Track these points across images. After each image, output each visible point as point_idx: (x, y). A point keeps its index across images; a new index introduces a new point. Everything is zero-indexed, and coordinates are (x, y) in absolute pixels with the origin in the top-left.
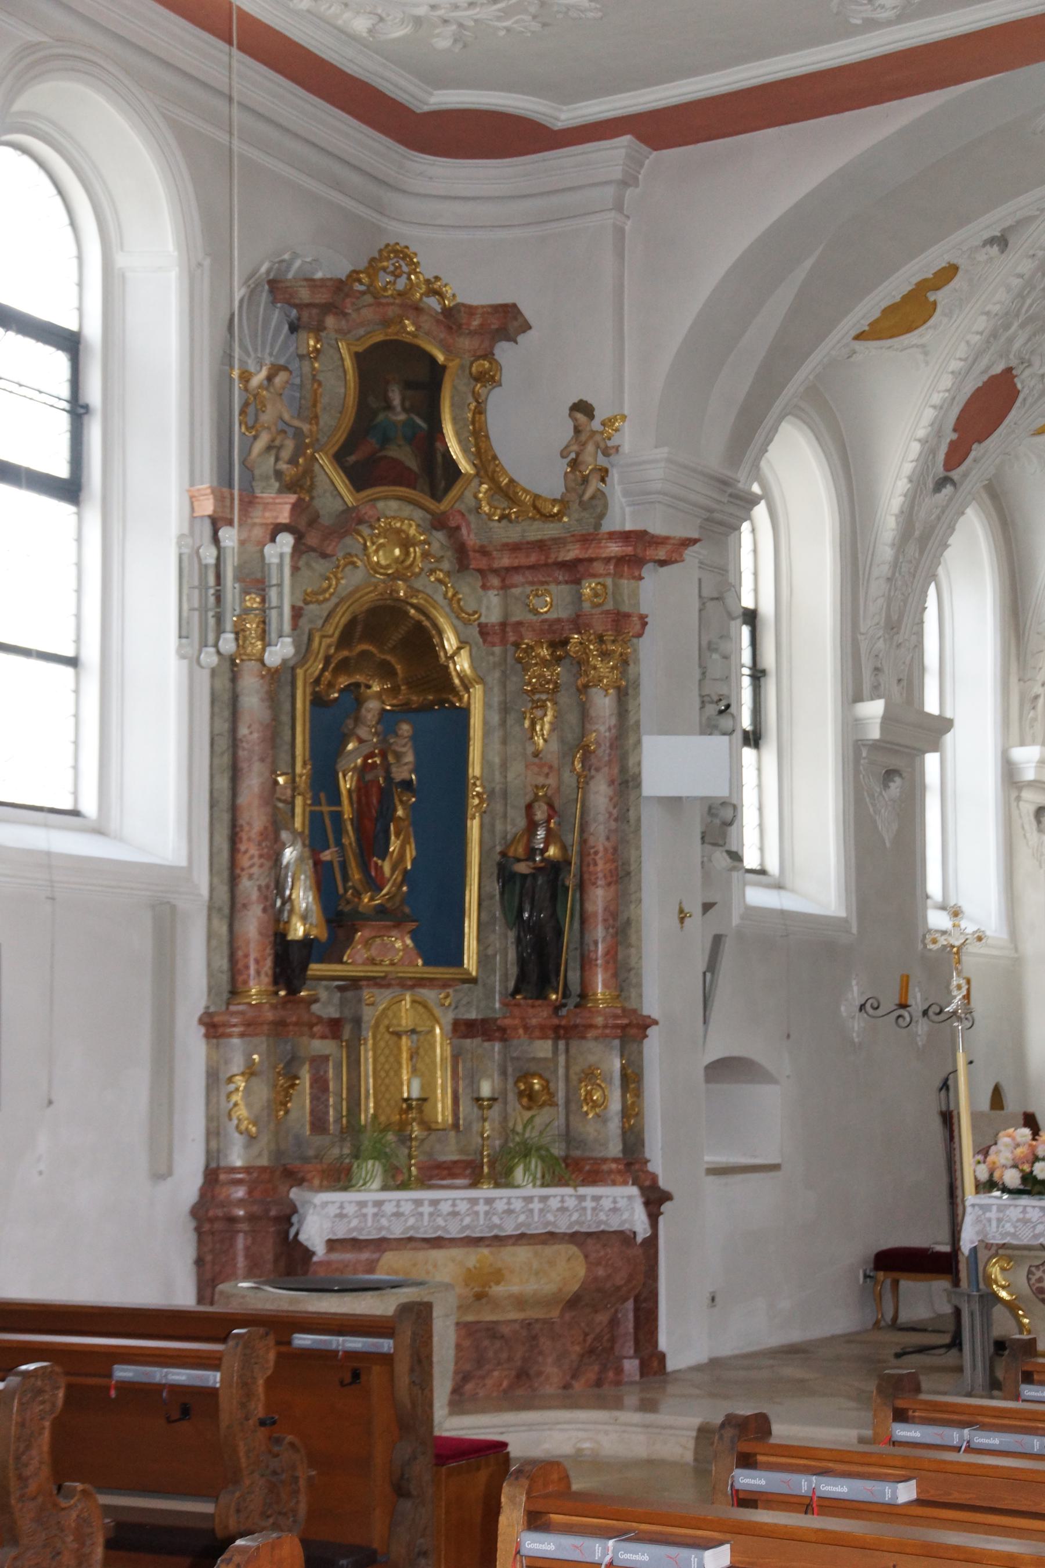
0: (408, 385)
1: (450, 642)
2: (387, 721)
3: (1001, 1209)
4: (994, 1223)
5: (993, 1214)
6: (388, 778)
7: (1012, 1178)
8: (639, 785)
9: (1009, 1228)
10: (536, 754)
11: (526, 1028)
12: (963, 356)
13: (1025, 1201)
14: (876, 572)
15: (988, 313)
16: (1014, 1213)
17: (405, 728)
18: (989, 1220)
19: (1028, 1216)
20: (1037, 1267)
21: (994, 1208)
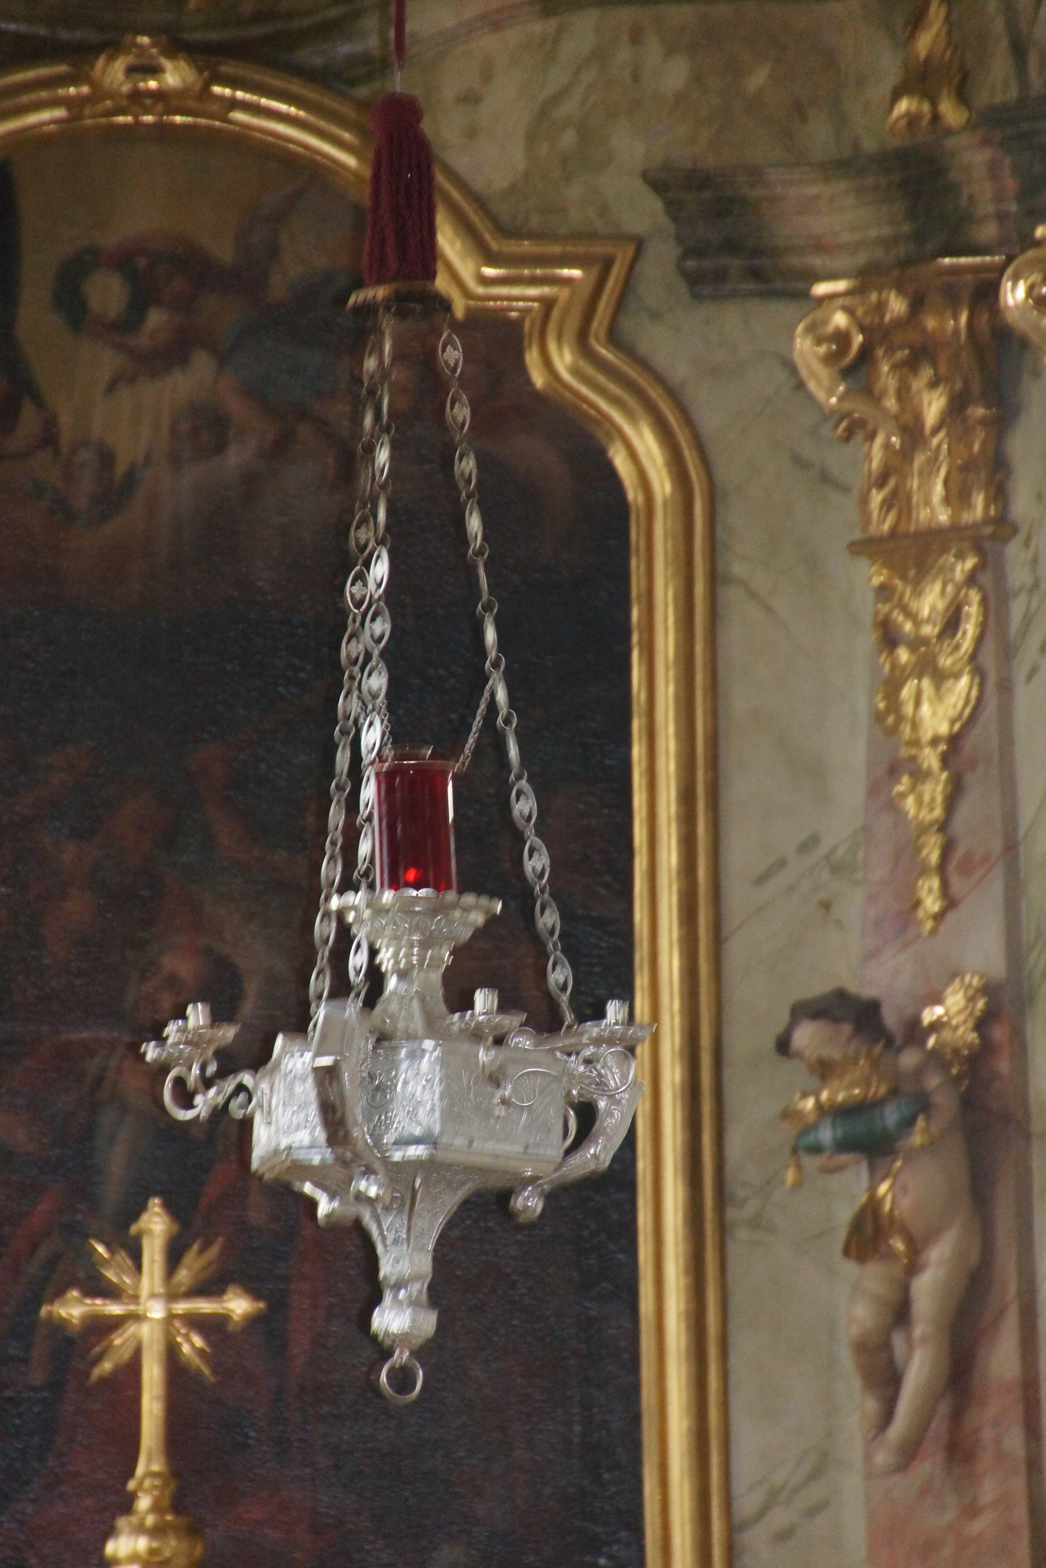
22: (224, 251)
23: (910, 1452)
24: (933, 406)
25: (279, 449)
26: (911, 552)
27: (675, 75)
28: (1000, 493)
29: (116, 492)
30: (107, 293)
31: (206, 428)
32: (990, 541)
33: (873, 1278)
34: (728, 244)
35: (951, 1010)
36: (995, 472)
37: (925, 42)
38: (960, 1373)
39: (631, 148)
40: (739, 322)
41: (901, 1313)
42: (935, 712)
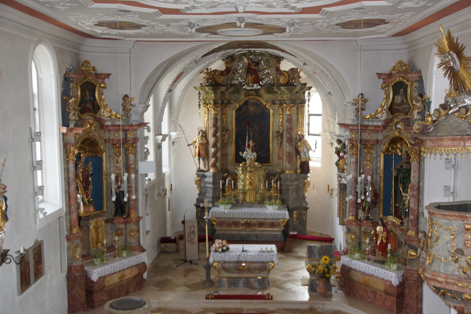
0: (90, 90)
1: (100, 145)
2: (87, 161)
6: (88, 174)
7: (220, 250)
8: (138, 172)
9: (219, 258)
10: (117, 166)
11: (119, 222)
13: (221, 254)
14: (159, 109)
17: (91, 163)
26: (280, 114)
29: (251, 112)
31: (255, 109)
32: (283, 114)
34: (274, 103)
35: (281, 131)
38: (281, 144)
39: (270, 99)
40: (274, 105)
42: (281, 120)
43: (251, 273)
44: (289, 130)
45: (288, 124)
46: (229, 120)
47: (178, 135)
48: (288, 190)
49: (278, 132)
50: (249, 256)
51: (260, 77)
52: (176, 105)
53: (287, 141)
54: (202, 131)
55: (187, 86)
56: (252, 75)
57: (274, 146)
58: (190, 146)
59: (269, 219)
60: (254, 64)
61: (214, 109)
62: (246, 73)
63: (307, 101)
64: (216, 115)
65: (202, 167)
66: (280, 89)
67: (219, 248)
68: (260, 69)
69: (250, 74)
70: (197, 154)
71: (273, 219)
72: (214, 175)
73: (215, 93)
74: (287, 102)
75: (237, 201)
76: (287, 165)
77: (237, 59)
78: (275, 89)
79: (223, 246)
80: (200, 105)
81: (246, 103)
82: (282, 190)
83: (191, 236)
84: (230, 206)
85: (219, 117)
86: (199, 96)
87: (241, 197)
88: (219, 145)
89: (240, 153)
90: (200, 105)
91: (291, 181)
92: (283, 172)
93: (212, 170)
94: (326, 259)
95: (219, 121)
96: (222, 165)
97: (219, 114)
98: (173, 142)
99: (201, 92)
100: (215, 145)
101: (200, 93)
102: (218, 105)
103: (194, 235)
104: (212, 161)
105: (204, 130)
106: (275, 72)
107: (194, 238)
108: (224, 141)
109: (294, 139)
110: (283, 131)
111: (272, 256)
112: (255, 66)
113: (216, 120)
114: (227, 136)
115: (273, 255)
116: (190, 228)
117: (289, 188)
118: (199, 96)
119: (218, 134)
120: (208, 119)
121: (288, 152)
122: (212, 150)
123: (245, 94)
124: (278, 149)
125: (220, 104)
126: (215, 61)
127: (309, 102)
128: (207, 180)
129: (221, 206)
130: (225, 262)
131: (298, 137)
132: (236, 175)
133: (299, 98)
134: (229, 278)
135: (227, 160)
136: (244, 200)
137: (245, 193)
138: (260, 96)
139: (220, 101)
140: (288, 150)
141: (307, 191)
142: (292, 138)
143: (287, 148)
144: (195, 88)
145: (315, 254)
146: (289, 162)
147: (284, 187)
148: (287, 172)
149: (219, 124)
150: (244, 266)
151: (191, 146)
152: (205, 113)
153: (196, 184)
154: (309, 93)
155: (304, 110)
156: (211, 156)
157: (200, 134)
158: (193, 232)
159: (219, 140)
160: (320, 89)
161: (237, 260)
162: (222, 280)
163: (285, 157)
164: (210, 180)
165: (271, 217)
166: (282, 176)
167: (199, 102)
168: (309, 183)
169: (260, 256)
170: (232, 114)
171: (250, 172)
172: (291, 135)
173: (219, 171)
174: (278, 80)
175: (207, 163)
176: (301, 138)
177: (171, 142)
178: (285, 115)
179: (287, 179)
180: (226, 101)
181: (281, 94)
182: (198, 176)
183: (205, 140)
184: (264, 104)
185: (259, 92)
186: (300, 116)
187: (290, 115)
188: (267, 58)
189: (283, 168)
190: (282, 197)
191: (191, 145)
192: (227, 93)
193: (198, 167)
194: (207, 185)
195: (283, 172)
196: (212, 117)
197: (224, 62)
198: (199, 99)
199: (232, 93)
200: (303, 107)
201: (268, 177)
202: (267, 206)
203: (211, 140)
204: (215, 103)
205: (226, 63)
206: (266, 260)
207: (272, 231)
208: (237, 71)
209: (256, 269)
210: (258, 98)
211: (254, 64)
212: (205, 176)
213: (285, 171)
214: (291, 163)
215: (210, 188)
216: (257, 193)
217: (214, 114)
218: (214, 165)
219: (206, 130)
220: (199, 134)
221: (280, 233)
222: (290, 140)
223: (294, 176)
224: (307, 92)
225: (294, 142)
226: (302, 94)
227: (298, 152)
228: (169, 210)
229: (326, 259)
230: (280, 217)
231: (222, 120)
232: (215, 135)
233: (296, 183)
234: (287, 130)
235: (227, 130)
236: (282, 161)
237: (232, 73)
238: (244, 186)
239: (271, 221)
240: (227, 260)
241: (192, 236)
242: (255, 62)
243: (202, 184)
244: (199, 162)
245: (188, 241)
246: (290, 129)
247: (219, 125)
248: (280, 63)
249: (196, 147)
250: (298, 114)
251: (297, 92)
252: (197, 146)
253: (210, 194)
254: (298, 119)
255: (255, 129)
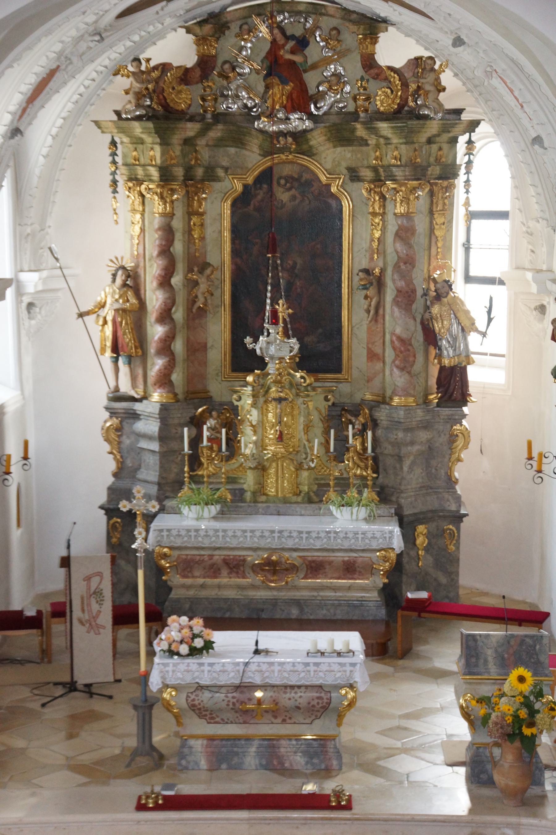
3: (175, 665)
4: (171, 673)
5: (170, 668)
7: (184, 649)
9: (179, 675)
12: (44, 65)
13: (190, 660)
15: (62, 42)
16: (182, 667)
18: (167, 672)
19: (190, 668)
20: (192, 693)
21: (171, 665)
22: (296, 176)
23: (370, 322)
24: (377, 198)
25: (302, 201)
26: (374, 214)
27: (349, 155)
28: (384, 209)
29: (283, 206)
30: (283, 182)
31: (294, 198)
33: (367, 302)
34: (354, 175)
35: (377, 270)
36: (383, 206)
37: (378, 153)
39: (344, 164)
40: (356, 185)
41: (370, 305)
42: (377, 234)
43: (284, 721)
44: (403, 267)
45: (399, 246)
46: (210, 232)
47: (45, 281)
48: (400, 459)
49: (367, 271)
50: (276, 668)
51: (312, 91)
52: (35, 181)
53: (396, 302)
54: (123, 268)
55: (71, 120)
56: (284, 82)
57: (355, 320)
58: (86, 318)
59: (340, 550)
60: (291, 44)
61: (162, 197)
62: (266, 77)
63: (463, 170)
64: (169, 216)
65: (125, 387)
66: (374, 131)
67: (181, 642)
68: (310, 62)
69: (276, 80)
70: (109, 344)
71: (352, 550)
72: (164, 409)
73: (165, 143)
74: (398, 173)
75: (239, 495)
76: (395, 378)
77: (234, 28)
78: (360, 131)
79: (195, 636)
80: (115, 183)
81: (266, 177)
82: (381, 458)
83: (89, 605)
84: (214, 509)
85: (177, 224)
86: (114, 154)
87: (249, 481)
88: (179, 314)
89: (248, 340)
90: (115, 183)
91: (408, 430)
92: (383, 400)
93: (156, 396)
94: (521, 679)
95: (178, 236)
96: (189, 379)
97: (179, 212)
98: (30, 305)
99: (117, 139)
100: (165, 316)
101: (113, 143)
102: (175, 186)
103: (100, 602)
104: (157, 368)
105: (129, 265)
106: (360, 72)
107: (100, 612)
108: (194, 302)
109: (419, 292)
110: (383, 271)
111: (348, 668)
112: (293, 52)
113: (168, 233)
114: (203, 287)
115: (353, 665)
116: (88, 579)
117: (404, 451)
118: (114, 154)
119: (177, 280)
120: (143, 230)
121: (400, 339)
122: (156, 332)
123: (261, 147)
124: (369, 329)
125: (184, 179)
126: (161, 35)
127: (468, 173)
128: (140, 426)
129: (185, 510)
130: (201, 687)
131: (433, 288)
132: (235, 410)
133: (438, 160)
134: (211, 739)
135: (204, 363)
136: (260, 490)
137: (261, 468)
138: (310, 153)
139: (179, 172)
140: (398, 331)
141: (459, 460)
142: (414, 291)
143: (396, 322)
144: (97, 123)
145: (486, 661)
146: (402, 369)
147: (388, 449)
148: (396, 400)
149: (178, 247)
150: (259, 702)
151: (90, 319)
152: (134, 211)
153: (107, 440)
154: (470, 142)
155: (451, 198)
156: (152, 349)
157: (119, 281)
158: (98, 593)
159: (181, 299)
160: (509, 125)
161: (237, 682)
162: (191, 747)
163: (389, 354)
164: (150, 426)
165: (346, 545)
166: (382, 414)
167: (114, 173)
168: (466, 435)
169: (312, 668)
170: (218, 211)
171: (280, 400)
172: (410, 282)
173: (181, 397)
174: (368, 99)
175: (140, 371)
176: (442, 291)
177: (24, 305)
178: (390, 217)
179: (396, 424)
180: (200, 172)
181: (377, 146)
182: (113, 413)
183: (133, 300)
184: (323, 179)
185: (307, 141)
186: (439, 219)
187: (407, 216)
188: (334, 22)
189: (384, 389)
190: (380, 480)
191: (88, 313)
192: (201, 142)
193: (112, 384)
194: (144, 444)
195: (384, 402)
196: (157, 221)
197: (191, 37)
198: (114, 162)
199: (219, 143)
200: (450, 188)
201: (338, 416)
202: (333, 508)
203: (155, 299)
204: (166, 176)
205: (201, 41)
206: (330, 680)
207: (350, 588)
208: (233, 69)
209: (298, 708)
210: (304, 160)
211: (291, 44)
212: (135, 416)
213: (391, 399)
214: (409, 373)
215: (153, 452)
216: (299, 467)
217: (163, 215)
218: (165, 380)
219: (137, 266)
220: (114, 280)
221: (374, 595)
222: (406, 298)
223: (420, 413)
224: (463, 139)
225: (418, 305)
226: (445, 146)
227: (431, 338)
228: (19, 525)
229: (521, 679)
230: (374, 545)
231: (189, 231)
232: (165, 282)
233: (423, 436)
234: (396, 267)
235: (204, 266)
236: (379, 365)
237: (220, 75)
238: (261, 445)
239: (346, 556)
240: (205, 680)
241: (95, 607)
242: (293, 37)
243: (126, 441)
244: (117, 370)
245: (81, 622)
246: (407, 262)
247: (178, 251)
248: (375, 40)
249: (105, 322)
250: (431, 213)
251: (430, 141)
252: (109, 318)
253: (150, 472)
254: (432, 230)
255: (295, 263)
